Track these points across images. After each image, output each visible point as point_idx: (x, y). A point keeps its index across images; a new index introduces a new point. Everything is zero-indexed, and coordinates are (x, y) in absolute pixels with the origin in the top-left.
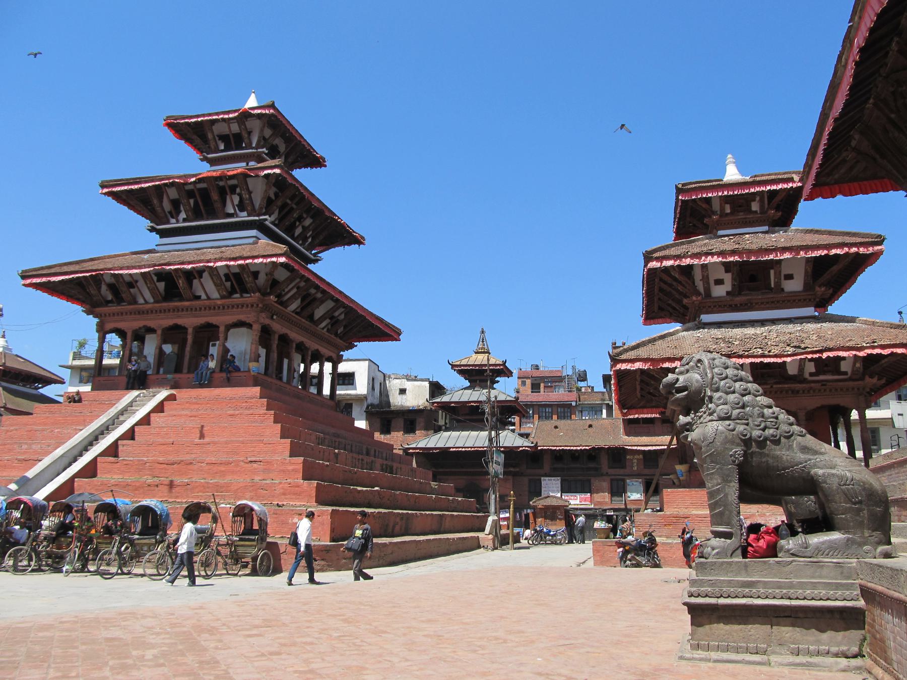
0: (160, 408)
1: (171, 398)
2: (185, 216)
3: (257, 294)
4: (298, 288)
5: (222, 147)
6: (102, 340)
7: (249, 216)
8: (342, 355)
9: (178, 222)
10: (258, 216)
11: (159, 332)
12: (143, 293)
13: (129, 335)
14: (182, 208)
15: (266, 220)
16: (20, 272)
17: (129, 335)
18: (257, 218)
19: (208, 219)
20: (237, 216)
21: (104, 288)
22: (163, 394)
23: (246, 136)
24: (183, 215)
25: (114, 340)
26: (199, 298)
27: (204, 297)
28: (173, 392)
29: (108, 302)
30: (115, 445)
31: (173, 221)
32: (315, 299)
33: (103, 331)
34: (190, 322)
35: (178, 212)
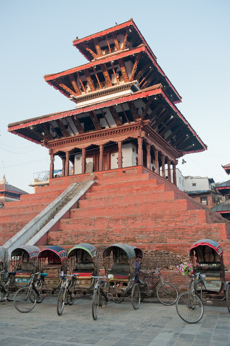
0: (90, 190)
1: (95, 184)
2: (90, 90)
3: (140, 119)
4: (157, 120)
5: (104, 53)
7: (125, 82)
8: (178, 160)
10: (131, 81)
11: (83, 151)
12: (73, 130)
13: (67, 156)
14: (88, 86)
17: (67, 156)
18: (130, 83)
20: (119, 84)
22: (92, 182)
23: (117, 43)
24: (89, 89)
25: (58, 160)
28: (97, 181)
29: (54, 138)
30: (69, 211)
32: (164, 128)
33: (53, 155)
34: (100, 142)
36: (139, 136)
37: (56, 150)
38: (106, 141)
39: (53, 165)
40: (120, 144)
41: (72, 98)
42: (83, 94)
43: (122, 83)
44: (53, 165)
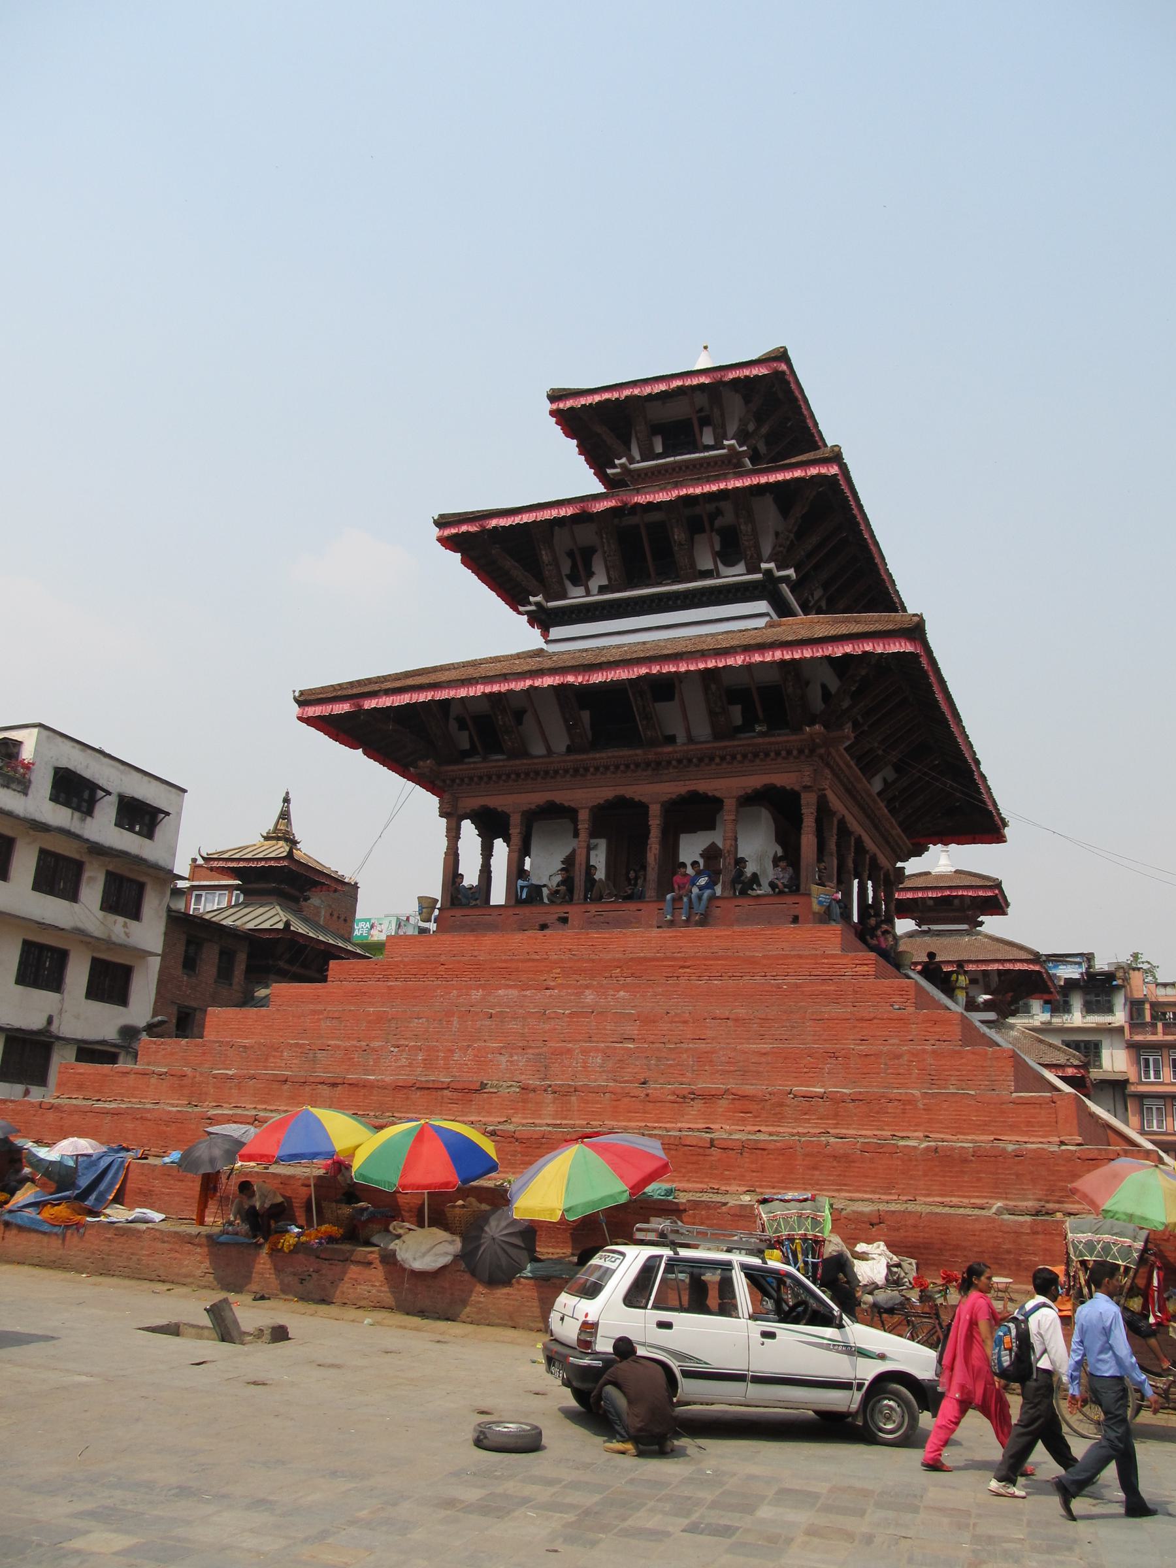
5: (659, 449)
6: (454, 835)
7: (749, 572)
9: (588, 594)
11: (584, 815)
15: (786, 579)
16: (297, 694)
19: (660, 584)
20: (719, 577)
21: (453, 725)
26: (671, 739)
27: (681, 738)
29: (465, 754)
31: (580, 591)
33: (452, 815)
35: (590, 574)
36: (809, 784)
37: (476, 802)
38: (671, 788)
39: (452, 857)
40: (730, 804)
41: (533, 608)
42: (577, 597)
43: (736, 574)
44: (456, 855)
